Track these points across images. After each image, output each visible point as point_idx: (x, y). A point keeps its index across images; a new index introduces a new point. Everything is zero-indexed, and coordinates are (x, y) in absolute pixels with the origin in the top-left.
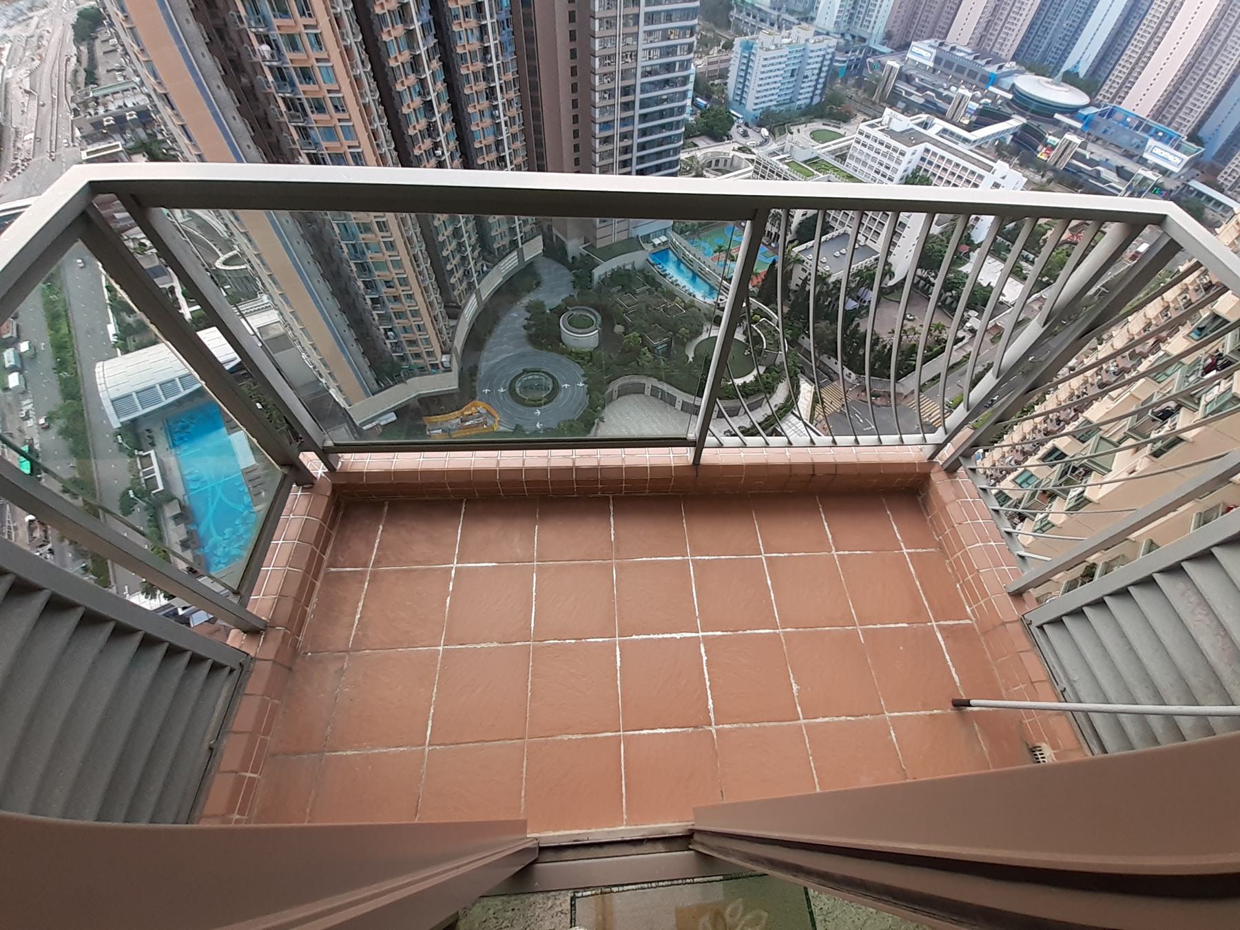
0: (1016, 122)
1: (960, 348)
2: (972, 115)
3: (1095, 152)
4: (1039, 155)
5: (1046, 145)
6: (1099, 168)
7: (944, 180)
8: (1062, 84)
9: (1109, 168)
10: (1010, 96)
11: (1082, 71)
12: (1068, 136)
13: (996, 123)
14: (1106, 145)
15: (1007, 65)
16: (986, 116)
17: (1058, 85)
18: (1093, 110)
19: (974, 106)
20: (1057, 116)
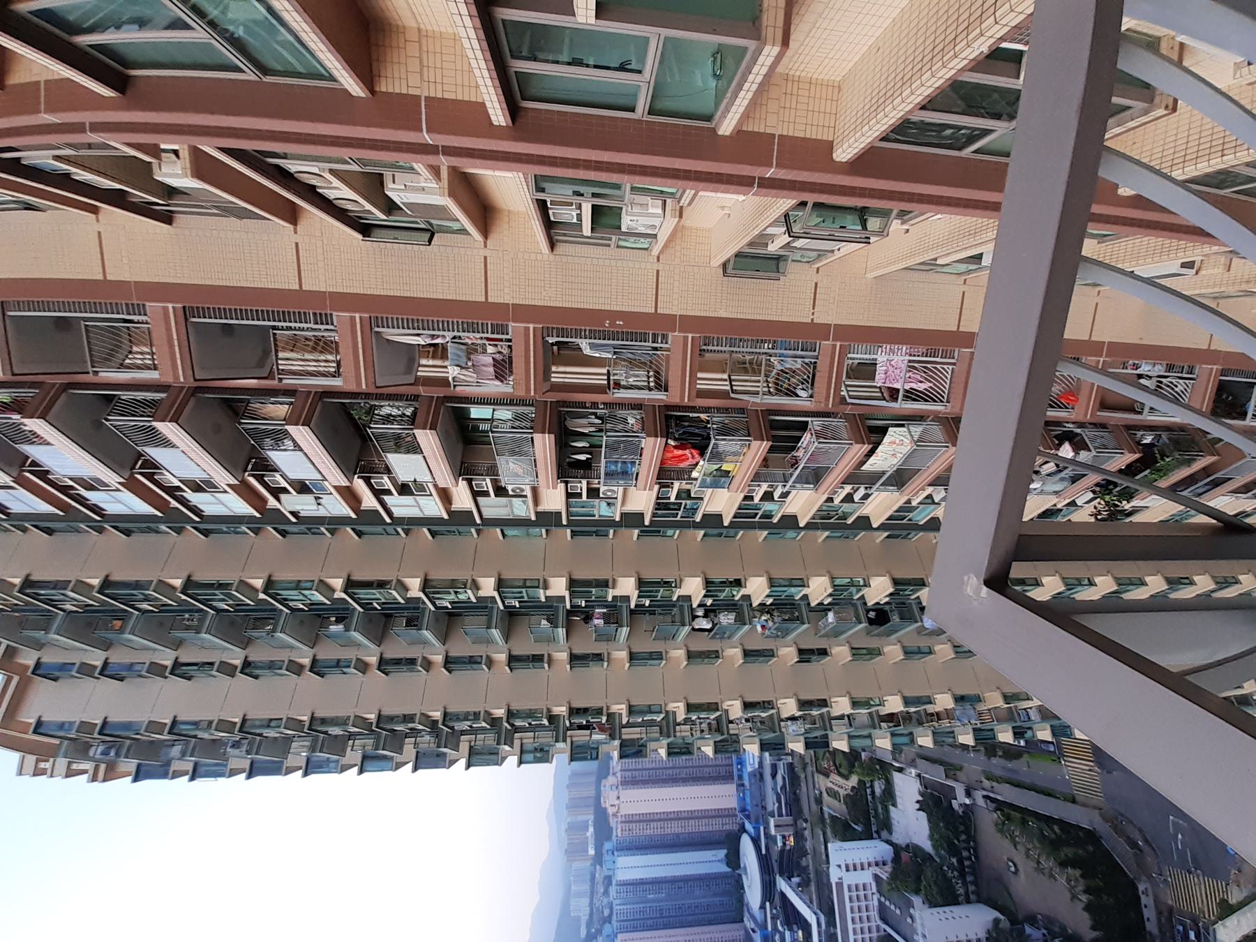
0: (782, 885)
1: (993, 792)
2: (794, 932)
3: (772, 805)
4: (792, 844)
5: (784, 844)
6: (779, 791)
7: (862, 925)
8: (742, 865)
9: (775, 783)
10: (768, 904)
11: (722, 853)
12: (773, 831)
13: (789, 900)
14: (763, 798)
15: (748, 926)
16: (792, 918)
17: (745, 868)
18: (748, 826)
19: (787, 934)
20: (764, 852)
